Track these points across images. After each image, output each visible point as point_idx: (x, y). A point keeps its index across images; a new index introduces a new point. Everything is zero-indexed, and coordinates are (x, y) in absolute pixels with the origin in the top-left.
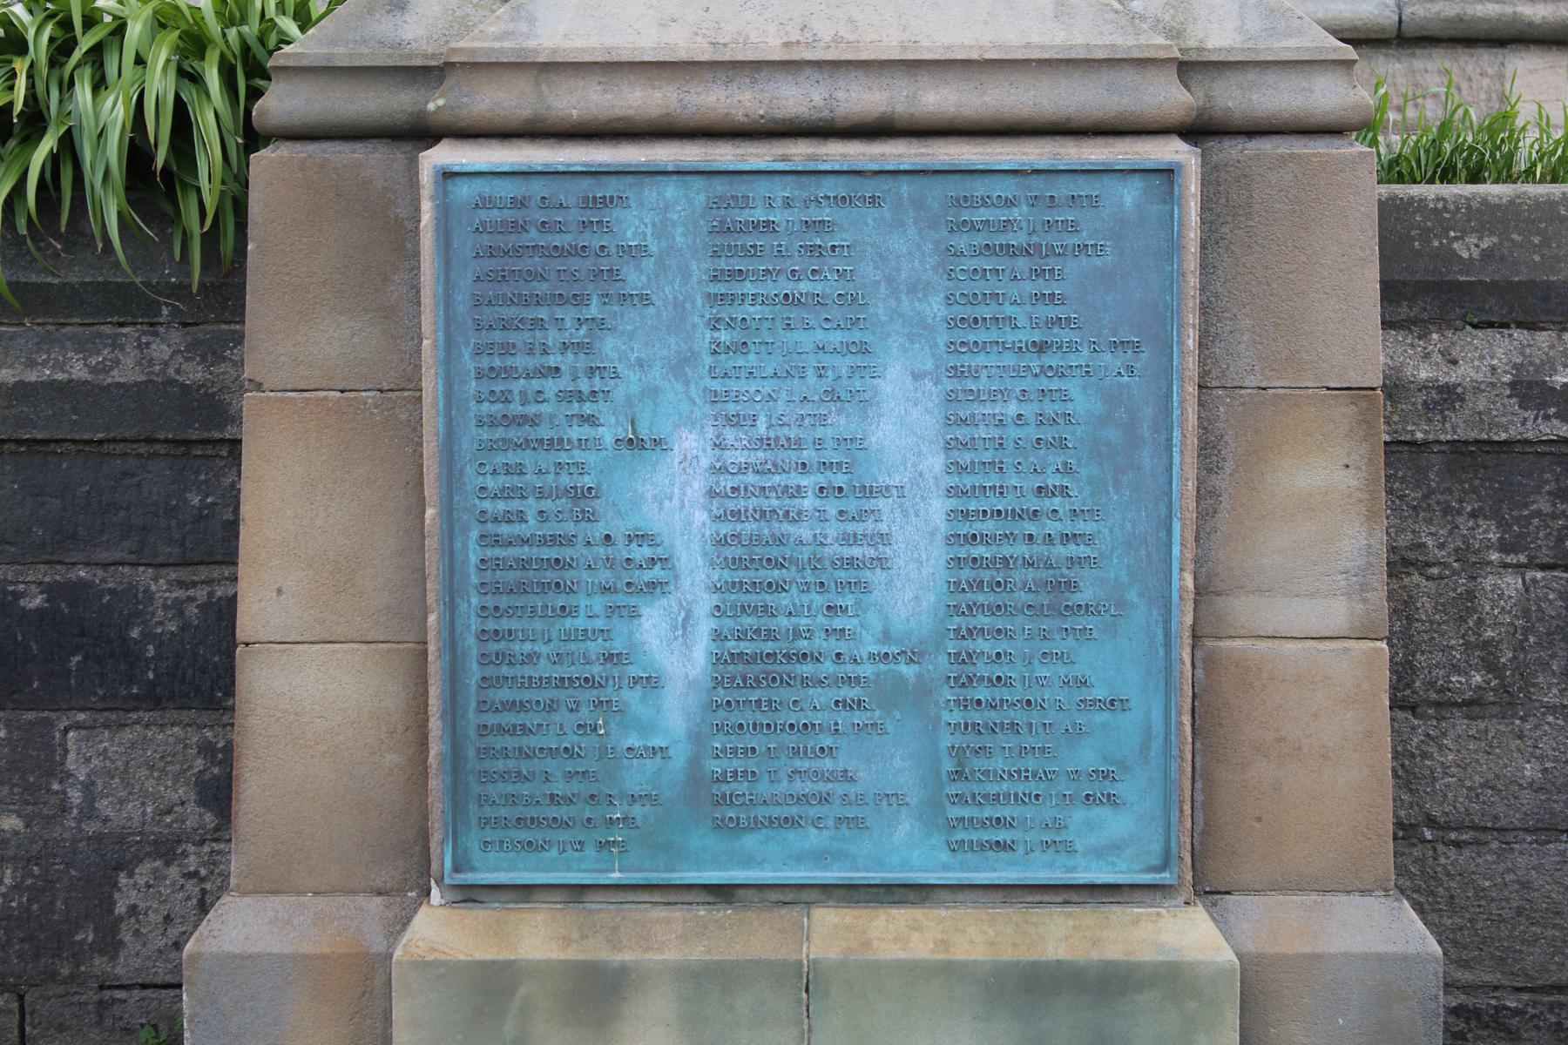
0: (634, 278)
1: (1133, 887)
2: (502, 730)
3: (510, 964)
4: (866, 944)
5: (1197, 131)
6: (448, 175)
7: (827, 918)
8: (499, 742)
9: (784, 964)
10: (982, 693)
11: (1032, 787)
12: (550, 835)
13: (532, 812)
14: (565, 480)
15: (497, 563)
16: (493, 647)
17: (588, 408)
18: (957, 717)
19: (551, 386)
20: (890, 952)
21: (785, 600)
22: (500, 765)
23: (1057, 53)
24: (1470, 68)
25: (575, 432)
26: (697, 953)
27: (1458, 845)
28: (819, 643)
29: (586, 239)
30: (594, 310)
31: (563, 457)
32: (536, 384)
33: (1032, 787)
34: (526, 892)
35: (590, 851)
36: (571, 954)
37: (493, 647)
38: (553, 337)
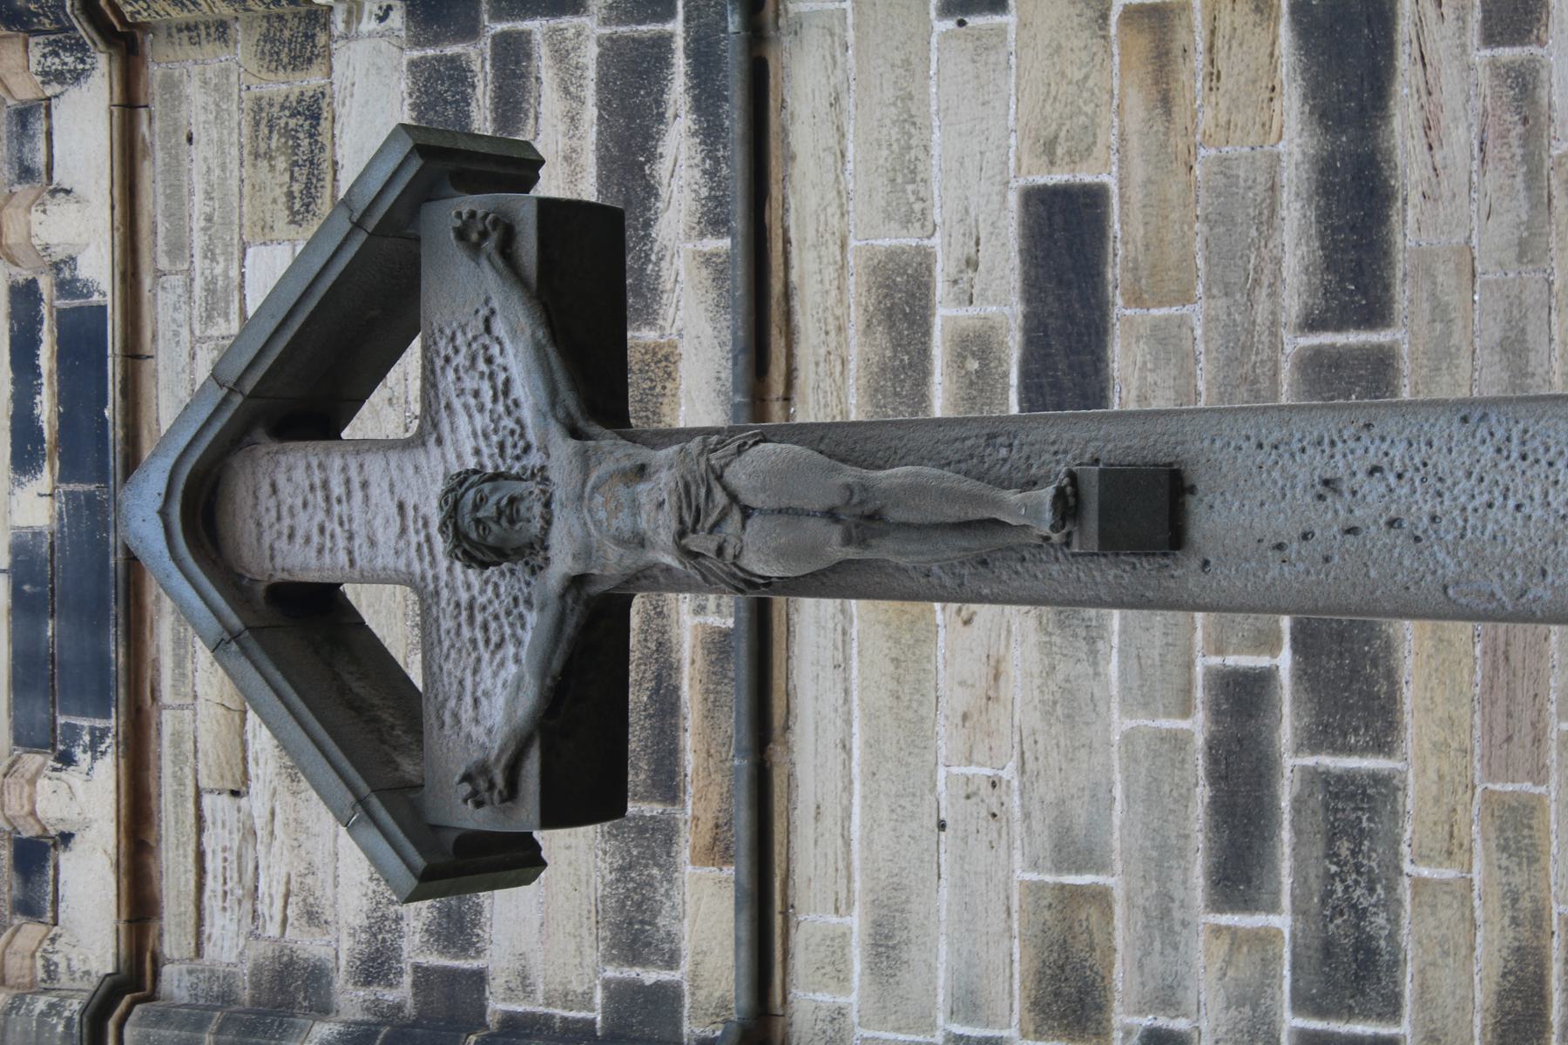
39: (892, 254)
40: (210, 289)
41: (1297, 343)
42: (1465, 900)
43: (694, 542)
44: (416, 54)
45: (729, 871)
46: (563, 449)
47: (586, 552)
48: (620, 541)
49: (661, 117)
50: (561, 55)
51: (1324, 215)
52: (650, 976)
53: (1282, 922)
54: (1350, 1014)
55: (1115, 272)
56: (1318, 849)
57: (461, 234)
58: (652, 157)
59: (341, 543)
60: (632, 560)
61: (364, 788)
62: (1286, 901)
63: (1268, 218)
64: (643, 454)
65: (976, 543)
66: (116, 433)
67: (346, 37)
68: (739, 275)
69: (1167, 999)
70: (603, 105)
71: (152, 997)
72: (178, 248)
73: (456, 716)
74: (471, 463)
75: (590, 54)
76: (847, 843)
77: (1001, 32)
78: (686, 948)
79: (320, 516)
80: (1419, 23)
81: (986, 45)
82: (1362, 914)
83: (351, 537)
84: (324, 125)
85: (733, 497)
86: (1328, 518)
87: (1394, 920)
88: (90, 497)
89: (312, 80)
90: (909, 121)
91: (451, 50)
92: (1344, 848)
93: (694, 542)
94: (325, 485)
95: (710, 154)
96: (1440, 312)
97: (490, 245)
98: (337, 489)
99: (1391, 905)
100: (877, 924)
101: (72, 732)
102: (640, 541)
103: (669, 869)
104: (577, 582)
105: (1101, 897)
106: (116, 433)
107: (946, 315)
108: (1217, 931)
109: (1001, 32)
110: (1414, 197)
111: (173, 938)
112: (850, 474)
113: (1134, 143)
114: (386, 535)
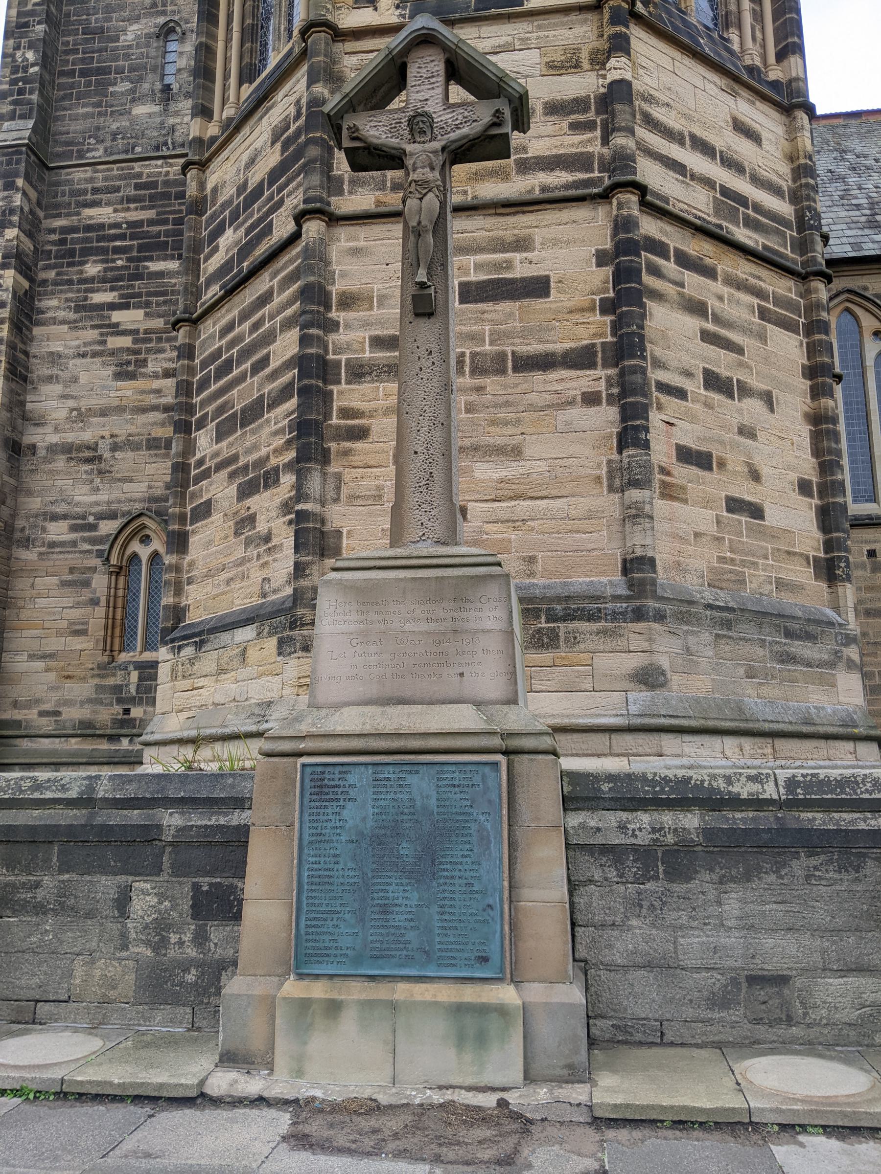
0: (352, 794)
1: (492, 979)
2: (314, 926)
3: (309, 998)
4: (412, 995)
5: (506, 753)
6: (304, 766)
7: (402, 986)
8: (311, 930)
9: (387, 1001)
10: (447, 917)
11: (462, 947)
12: (324, 958)
13: (319, 952)
14: (332, 852)
15: (313, 876)
16: (310, 901)
17: (338, 831)
18: (440, 924)
19: (329, 825)
20: (419, 998)
21: (391, 888)
22: (310, 937)
23: (314, 725)
24: (651, 738)
25: (334, 838)
26: (363, 996)
27: (610, 970)
28: (400, 901)
29: (341, 783)
30: (341, 803)
31: (332, 845)
32: (325, 824)
33: (462, 947)
34: (317, 976)
35: (335, 963)
36: (327, 996)
37: (310, 901)
38: (330, 811)
39: (533, 240)
40: (528, 39)
41: (509, 350)
42: (375, 399)
43: (413, 184)
44: (592, 97)
45: (373, 206)
46: (437, 145)
47: (412, 154)
48: (414, 163)
49: (572, 171)
50: (590, 141)
51: (541, 355)
52: (346, 187)
53: (367, 354)
54: (346, 372)
55: (526, 302)
56: (385, 363)
57: (498, 111)
58: (561, 170)
59: (417, 83)
60: (410, 167)
61: (351, 95)
62: (372, 355)
63: (541, 341)
64: (438, 169)
65: (415, 263)
66: (487, 13)
67: (598, 75)
68: (528, 197)
69: (348, 326)
70: (576, 154)
71: (334, 41)
72: (539, 27)
73: (371, 121)
74: (435, 120)
75: (590, 149)
76: (382, 239)
77: (591, 267)
78: (353, 197)
79: (425, 76)
80: (588, 376)
81: (587, 261)
82: (370, 374)
83: (419, 85)
84: (573, 70)
85: (425, 195)
86: (422, 352)
87: (369, 382)
88: (470, 7)
89: (586, 65)
90: (568, 242)
91: (593, 108)
92: (386, 369)
93: (413, 184)
94: (433, 77)
95: (562, 187)
96: (516, 385)
97: (495, 120)
98: (432, 80)
99: (373, 381)
100: (362, 249)
101: (405, 8)
102: (414, 170)
103: (373, 190)
104: (404, 152)
105: (371, 308)
106: (487, 13)
107: (517, 257)
108: (364, 338)
109: (591, 267)
110: (544, 377)
111: (350, 46)
112: (430, 227)
113: (561, 304)
114: (420, 96)
